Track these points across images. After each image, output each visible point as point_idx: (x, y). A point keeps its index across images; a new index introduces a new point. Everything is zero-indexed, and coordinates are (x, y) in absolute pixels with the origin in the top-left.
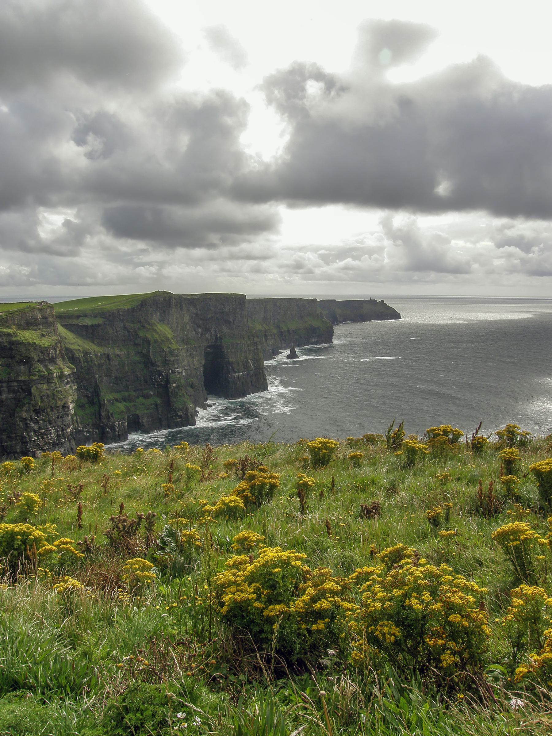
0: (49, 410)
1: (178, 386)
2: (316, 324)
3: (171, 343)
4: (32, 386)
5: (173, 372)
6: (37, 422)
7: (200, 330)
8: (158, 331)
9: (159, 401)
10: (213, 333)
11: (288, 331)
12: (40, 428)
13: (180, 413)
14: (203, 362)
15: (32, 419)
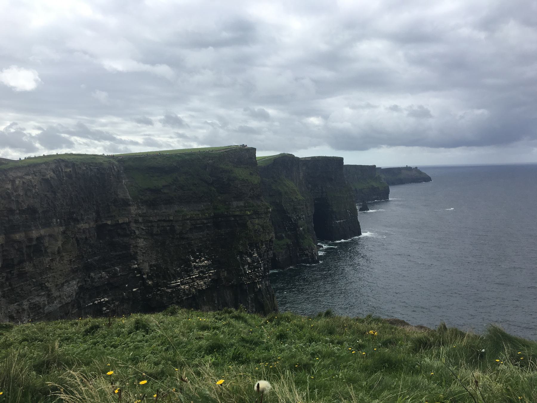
0: (260, 244)
1: (303, 230)
2: (375, 185)
3: (297, 195)
4: (248, 221)
5: (300, 218)
6: (251, 256)
7: (310, 186)
8: (287, 185)
9: (289, 242)
10: (320, 188)
11: (356, 190)
12: (253, 262)
13: (306, 252)
14: (313, 211)
15: (247, 252)
